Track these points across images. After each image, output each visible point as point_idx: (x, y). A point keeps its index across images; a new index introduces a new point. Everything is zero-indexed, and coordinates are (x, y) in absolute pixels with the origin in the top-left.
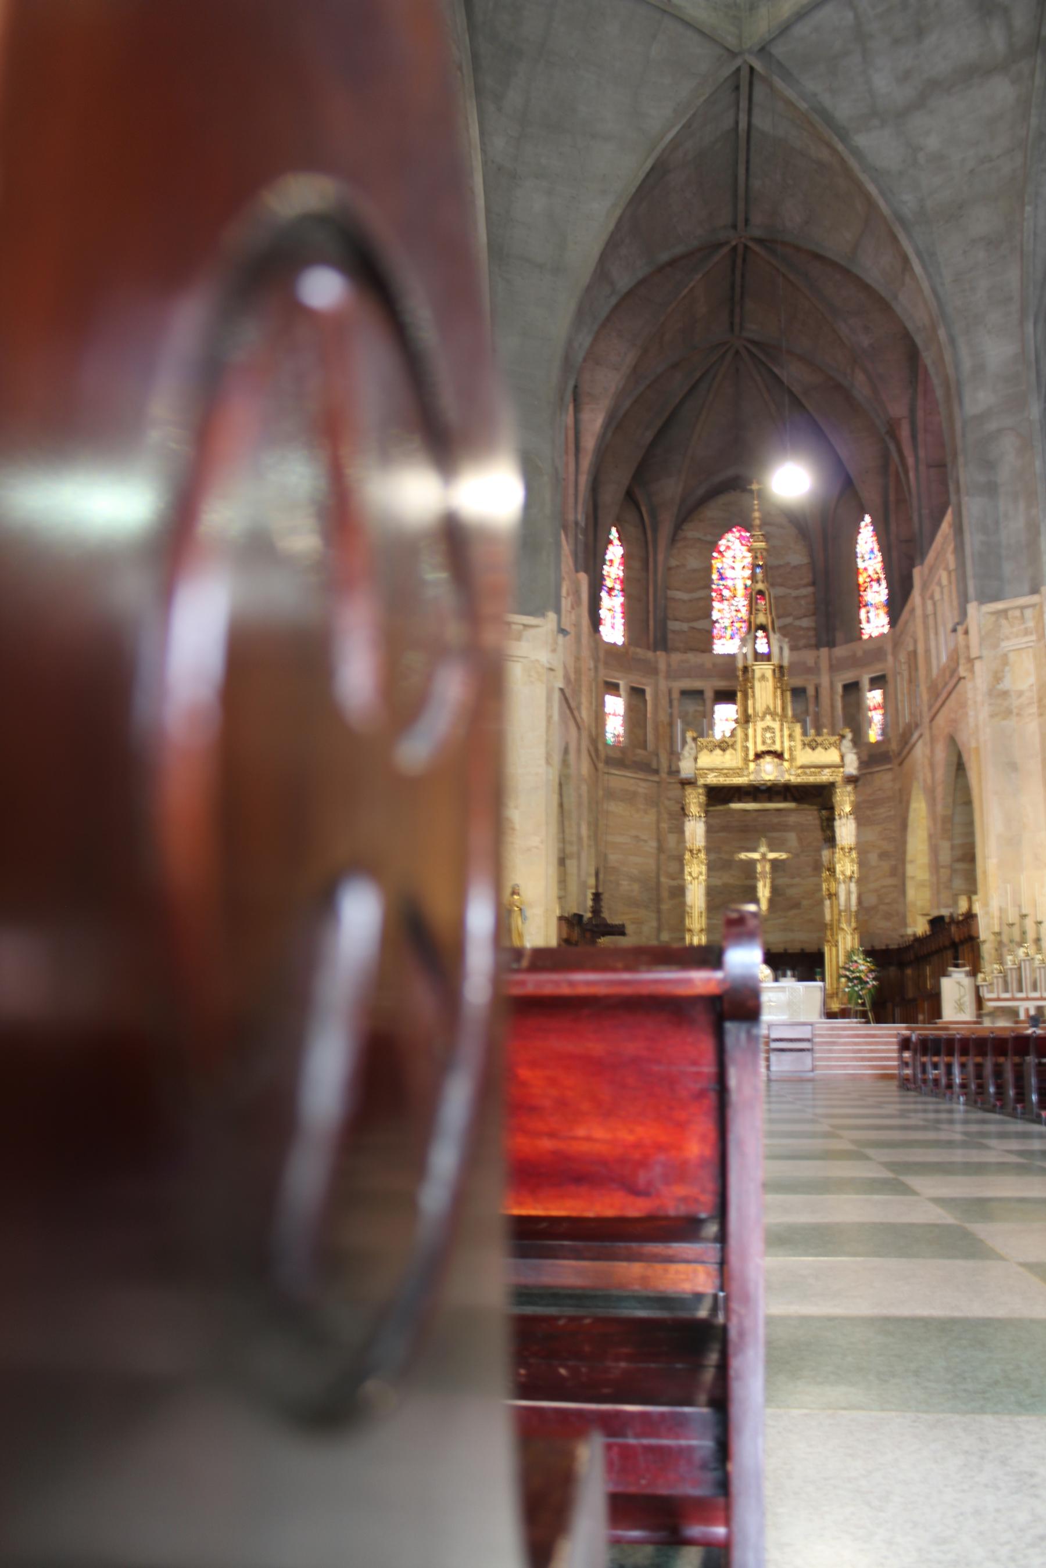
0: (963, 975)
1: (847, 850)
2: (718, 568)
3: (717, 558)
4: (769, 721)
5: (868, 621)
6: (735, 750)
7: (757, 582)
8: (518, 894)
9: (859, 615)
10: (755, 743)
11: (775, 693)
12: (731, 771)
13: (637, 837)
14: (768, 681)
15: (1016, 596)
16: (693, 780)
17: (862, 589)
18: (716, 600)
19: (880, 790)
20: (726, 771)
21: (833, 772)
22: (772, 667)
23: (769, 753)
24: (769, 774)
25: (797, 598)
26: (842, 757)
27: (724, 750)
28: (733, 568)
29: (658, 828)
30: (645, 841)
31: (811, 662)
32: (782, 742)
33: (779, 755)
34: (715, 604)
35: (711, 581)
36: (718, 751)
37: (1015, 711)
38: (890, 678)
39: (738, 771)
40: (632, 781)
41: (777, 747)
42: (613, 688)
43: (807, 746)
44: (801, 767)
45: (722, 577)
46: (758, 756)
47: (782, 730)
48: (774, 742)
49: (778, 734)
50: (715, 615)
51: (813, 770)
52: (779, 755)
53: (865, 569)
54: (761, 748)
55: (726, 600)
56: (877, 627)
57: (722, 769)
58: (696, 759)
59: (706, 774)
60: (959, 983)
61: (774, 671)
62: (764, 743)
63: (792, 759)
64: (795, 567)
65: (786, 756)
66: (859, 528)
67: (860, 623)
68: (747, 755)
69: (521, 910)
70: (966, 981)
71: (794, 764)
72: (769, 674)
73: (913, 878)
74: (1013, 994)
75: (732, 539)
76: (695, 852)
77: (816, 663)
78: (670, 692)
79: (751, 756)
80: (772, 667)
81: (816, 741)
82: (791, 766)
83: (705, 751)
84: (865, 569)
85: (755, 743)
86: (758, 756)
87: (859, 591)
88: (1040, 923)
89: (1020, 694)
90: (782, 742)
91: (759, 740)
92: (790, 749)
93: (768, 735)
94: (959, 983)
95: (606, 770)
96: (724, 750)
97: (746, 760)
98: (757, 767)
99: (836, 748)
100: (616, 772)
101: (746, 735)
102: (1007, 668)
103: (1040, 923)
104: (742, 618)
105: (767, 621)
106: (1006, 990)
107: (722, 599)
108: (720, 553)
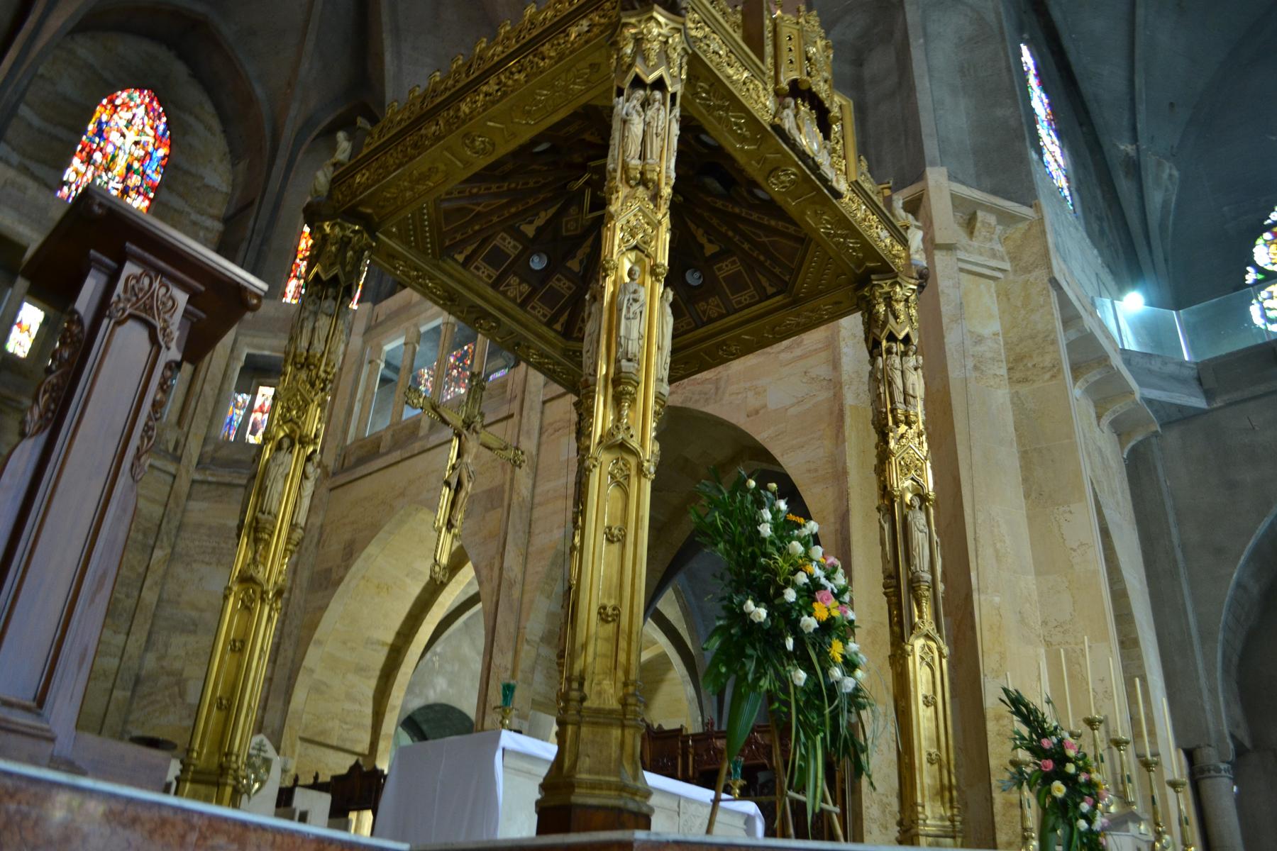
9: (286, 285)
17: (300, 256)
18: (79, 155)
25: (194, 223)
28: (123, 135)
34: (76, 162)
35: (85, 132)
45: (100, 133)
64: (207, 186)
73: (312, 671)
87: (296, 257)
107: (88, 161)
108: (111, 102)
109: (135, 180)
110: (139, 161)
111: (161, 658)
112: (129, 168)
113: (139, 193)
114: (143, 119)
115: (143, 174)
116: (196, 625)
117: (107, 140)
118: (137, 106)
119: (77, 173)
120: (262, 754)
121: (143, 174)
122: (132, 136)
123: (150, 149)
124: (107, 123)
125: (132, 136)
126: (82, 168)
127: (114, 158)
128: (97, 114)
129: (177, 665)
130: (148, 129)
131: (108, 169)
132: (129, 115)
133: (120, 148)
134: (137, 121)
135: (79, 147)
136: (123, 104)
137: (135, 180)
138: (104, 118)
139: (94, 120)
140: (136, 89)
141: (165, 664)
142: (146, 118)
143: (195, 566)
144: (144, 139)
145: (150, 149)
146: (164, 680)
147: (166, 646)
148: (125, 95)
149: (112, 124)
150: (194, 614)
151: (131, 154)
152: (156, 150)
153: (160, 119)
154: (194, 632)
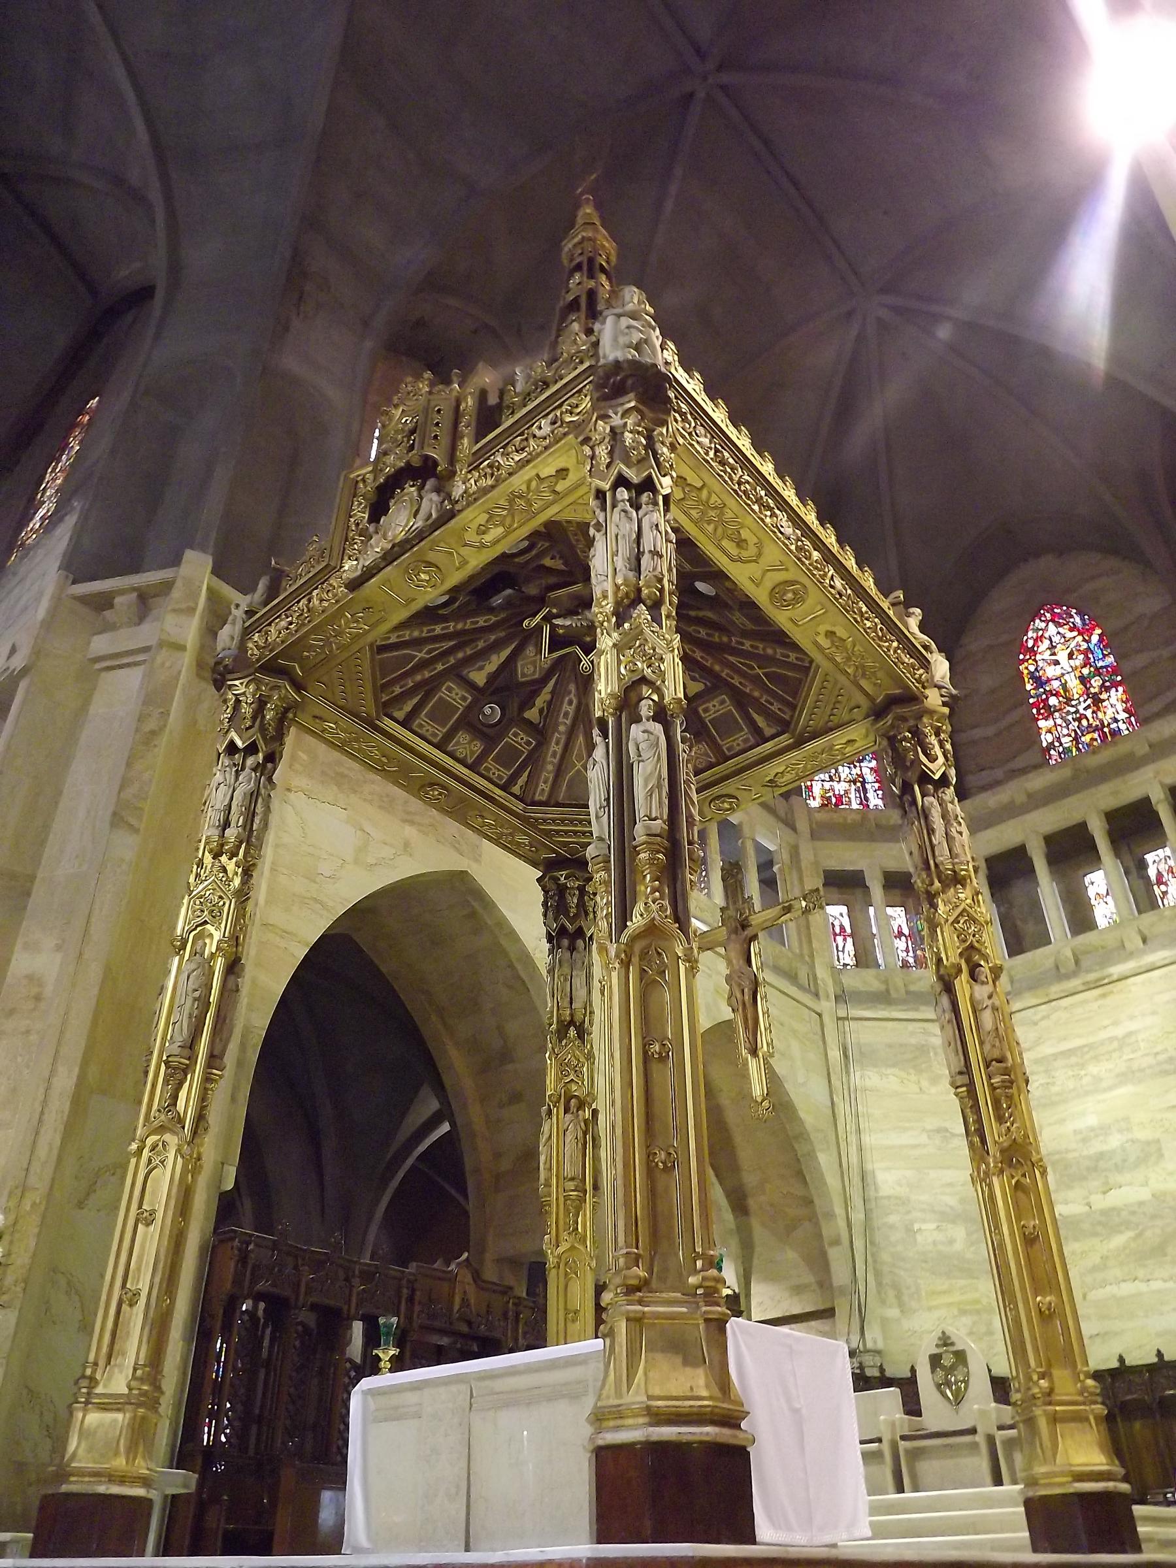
2: (1030, 673)
18: (1041, 717)
28: (1057, 663)
34: (1042, 724)
40: (911, 1026)
45: (1039, 682)
50: (1045, 739)
55: (1057, 711)
75: (1043, 625)
95: (842, 1013)
104: (1090, 725)
107: (1050, 712)
109: (1096, 682)
110: (1085, 666)
112: (1083, 680)
113: (1108, 689)
114: (1059, 633)
115: (1098, 672)
117: (1049, 680)
118: (1045, 630)
119: (1049, 731)
120: (952, 1349)
121: (1098, 672)
122: (1062, 656)
123: (1084, 646)
124: (1036, 669)
125: (1062, 656)
126: (1050, 723)
127: (1064, 686)
128: (1026, 672)
130: (1069, 635)
131: (1068, 701)
132: (1047, 643)
133: (1063, 675)
134: (1056, 639)
135: (1034, 711)
136: (1036, 641)
137: (1096, 682)
138: (1032, 668)
139: (1026, 680)
142: (1060, 629)
144: (1073, 644)
145: (1084, 646)
148: (1030, 634)
149: (1041, 664)
151: (1074, 669)
152: (1088, 642)
153: (1072, 617)
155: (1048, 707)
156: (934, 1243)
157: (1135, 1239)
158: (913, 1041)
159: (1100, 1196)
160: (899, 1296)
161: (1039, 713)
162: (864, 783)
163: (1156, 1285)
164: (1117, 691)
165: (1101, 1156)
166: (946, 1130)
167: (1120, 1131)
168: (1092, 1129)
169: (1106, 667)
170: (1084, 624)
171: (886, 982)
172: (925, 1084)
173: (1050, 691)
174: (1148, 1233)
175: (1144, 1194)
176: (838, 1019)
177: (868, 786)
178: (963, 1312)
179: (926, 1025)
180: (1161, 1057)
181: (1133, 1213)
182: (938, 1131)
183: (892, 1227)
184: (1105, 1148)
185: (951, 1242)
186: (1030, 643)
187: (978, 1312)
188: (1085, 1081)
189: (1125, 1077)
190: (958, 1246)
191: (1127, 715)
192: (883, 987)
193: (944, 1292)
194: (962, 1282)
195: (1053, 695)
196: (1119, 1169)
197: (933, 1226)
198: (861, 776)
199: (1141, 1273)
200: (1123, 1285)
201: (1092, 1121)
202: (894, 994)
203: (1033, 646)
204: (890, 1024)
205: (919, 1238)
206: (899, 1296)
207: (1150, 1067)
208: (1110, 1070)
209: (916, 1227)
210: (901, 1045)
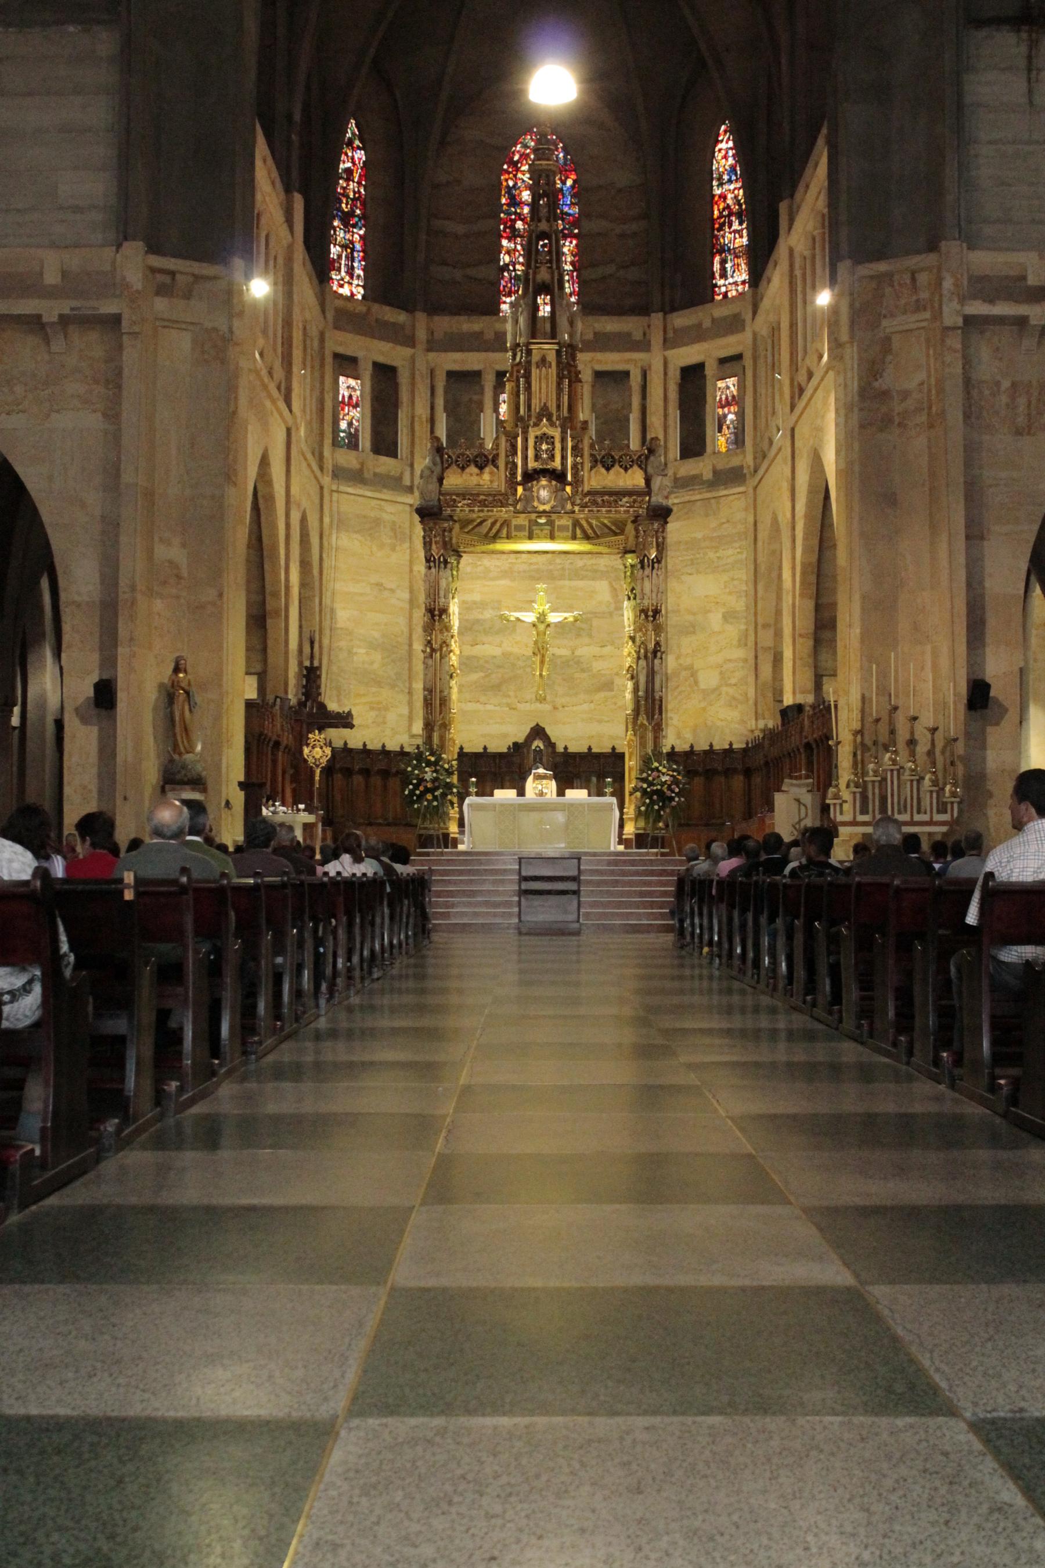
0: (804, 790)
1: (650, 613)
2: (508, 186)
3: (509, 173)
4: (545, 428)
5: (724, 275)
6: (497, 468)
7: (539, 221)
8: (185, 671)
10: (525, 458)
11: (559, 384)
12: (491, 499)
13: (379, 585)
14: (550, 367)
15: (908, 253)
16: (435, 510)
17: (717, 226)
19: (728, 521)
20: (482, 497)
21: (635, 501)
22: (556, 347)
23: (544, 472)
24: (549, 502)
25: (622, 236)
26: (648, 481)
27: (481, 468)
29: (411, 571)
30: (392, 591)
31: (638, 336)
32: (564, 458)
33: (559, 477)
36: (473, 469)
37: (897, 420)
38: (748, 361)
39: (501, 498)
40: (374, 503)
41: (557, 464)
42: (347, 364)
43: (600, 465)
44: (589, 493)
46: (530, 477)
47: (563, 440)
48: (552, 457)
49: (558, 446)
50: (505, 259)
51: (606, 498)
52: (559, 477)
53: (723, 197)
54: (532, 464)
56: (736, 283)
57: (478, 495)
58: (441, 480)
59: (455, 501)
60: (798, 801)
61: (558, 353)
62: (537, 457)
63: (577, 482)
65: (569, 478)
66: (718, 135)
67: (714, 278)
68: (514, 474)
69: (187, 693)
70: (807, 799)
71: (580, 489)
72: (552, 357)
74: (912, 816)
76: (437, 613)
77: (645, 334)
78: (432, 372)
79: (519, 478)
80: (556, 347)
81: (612, 457)
82: (575, 492)
83: (454, 467)
84: (723, 197)
85: (525, 458)
86: (530, 477)
87: (713, 229)
88: (915, 719)
89: (905, 395)
90: (564, 458)
91: (531, 453)
92: (575, 466)
93: (544, 447)
94: (798, 801)
95: (334, 487)
96: (481, 468)
97: (512, 484)
98: (527, 493)
99: (640, 466)
100: (350, 490)
101: (514, 447)
102: (889, 358)
103: (915, 719)
105: (553, 278)
106: (864, 811)
111: (678, 658)
116: (694, 627)
119: (508, 252)
124: (514, 186)
128: (505, 184)
129: (688, 661)
135: (502, 227)
136: (521, 156)
138: (511, 183)
140: (526, 135)
141: (681, 661)
143: (683, 577)
146: (684, 673)
147: (679, 646)
150: (690, 618)
152: (564, 183)
153: (557, 149)
154: (694, 633)
155: (513, 228)
156: (363, 663)
157: (484, 678)
158: (372, 514)
159: (469, 647)
160: (338, 696)
161: (504, 231)
162: (353, 250)
163: (489, 707)
164: (571, 242)
165: (478, 621)
166: (382, 585)
167: (493, 608)
168: (475, 603)
169: (570, 215)
170: (565, 164)
171: (362, 464)
172: (375, 549)
173: (520, 214)
174: (494, 676)
175: (497, 651)
176: (332, 491)
177: (356, 254)
178: (372, 709)
179: (383, 503)
180: (533, 567)
181: (487, 662)
182: (377, 585)
183: (341, 649)
184: (480, 617)
185: (372, 663)
186: (516, 158)
187: (379, 709)
188: (480, 569)
189: (507, 574)
190: (376, 666)
191: (571, 268)
192: (358, 466)
193: (364, 695)
194: (374, 690)
195: (522, 220)
196: (486, 632)
197: (362, 651)
198: (352, 242)
199: (483, 699)
200: (469, 704)
201: (477, 597)
202: (366, 475)
203: (518, 162)
204: (360, 499)
205: (355, 658)
206: (338, 696)
207: (524, 571)
208: (498, 567)
209: (355, 650)
210: (365, 517)
